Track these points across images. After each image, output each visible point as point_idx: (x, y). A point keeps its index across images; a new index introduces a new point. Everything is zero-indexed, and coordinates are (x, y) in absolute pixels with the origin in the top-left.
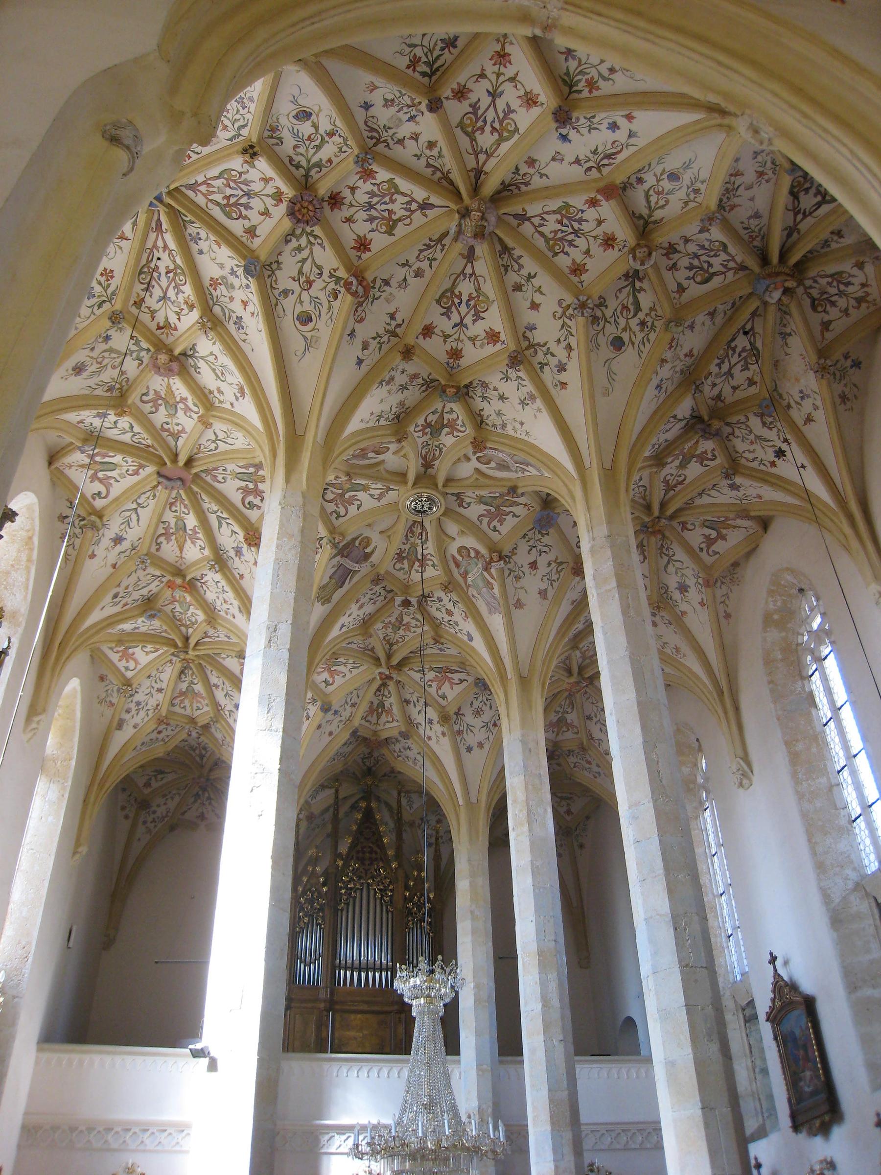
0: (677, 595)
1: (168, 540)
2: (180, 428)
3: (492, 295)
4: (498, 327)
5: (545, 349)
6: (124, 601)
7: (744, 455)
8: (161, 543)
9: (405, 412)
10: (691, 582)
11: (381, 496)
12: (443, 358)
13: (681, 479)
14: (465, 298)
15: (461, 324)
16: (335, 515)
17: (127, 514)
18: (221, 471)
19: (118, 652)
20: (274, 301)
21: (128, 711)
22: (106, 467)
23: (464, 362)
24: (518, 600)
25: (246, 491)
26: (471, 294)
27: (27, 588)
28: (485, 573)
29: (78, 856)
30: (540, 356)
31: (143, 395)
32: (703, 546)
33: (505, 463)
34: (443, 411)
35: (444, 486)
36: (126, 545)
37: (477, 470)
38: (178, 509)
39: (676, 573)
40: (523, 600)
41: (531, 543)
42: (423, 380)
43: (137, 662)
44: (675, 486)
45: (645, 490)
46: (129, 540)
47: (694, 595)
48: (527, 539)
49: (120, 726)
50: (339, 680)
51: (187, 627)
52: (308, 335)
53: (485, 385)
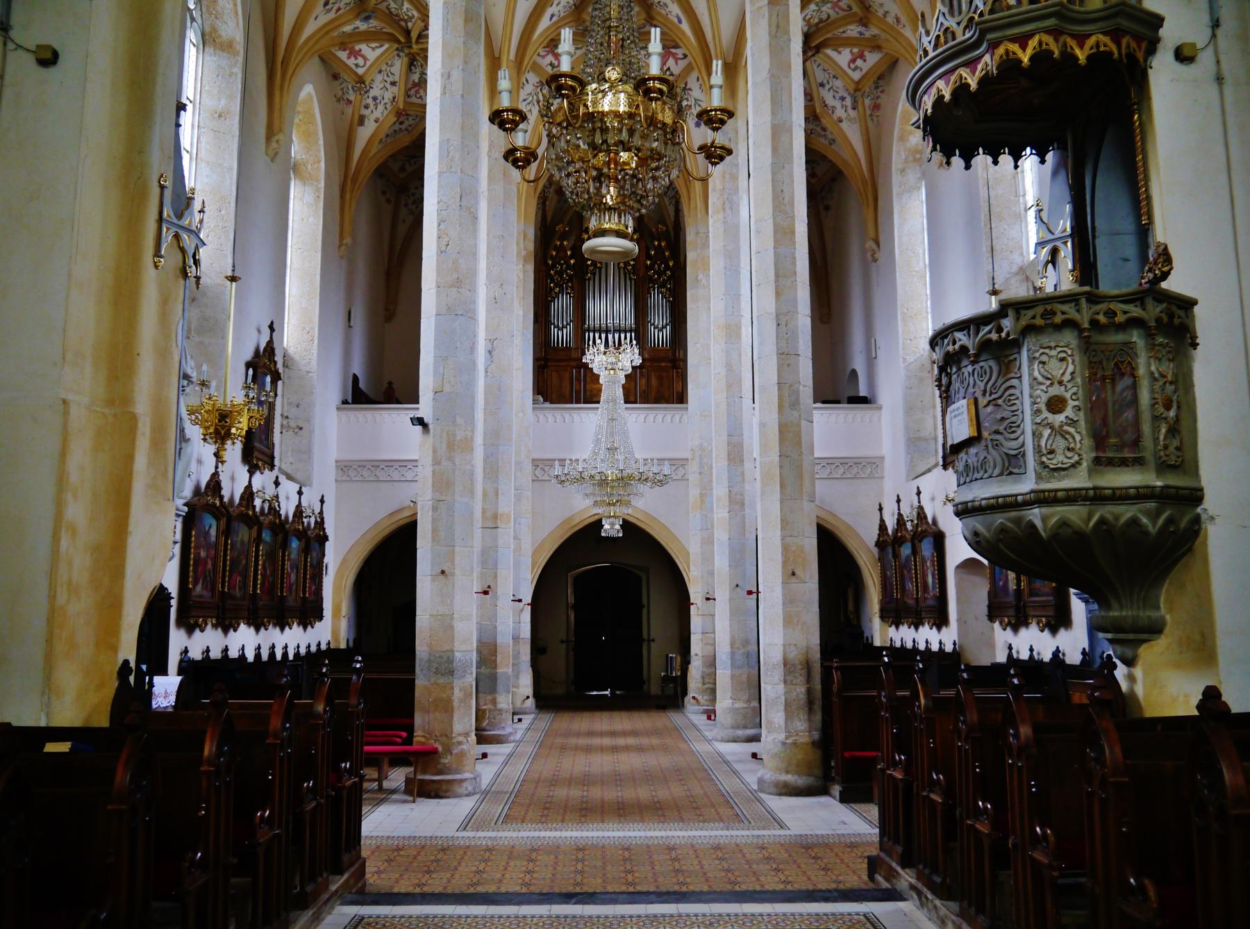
6: (336, 7)
21: (367, 107)
27: (237, 13)
29: (343, 248)
43: (365, 59)
49: (362, 120)
51: (406, 21)
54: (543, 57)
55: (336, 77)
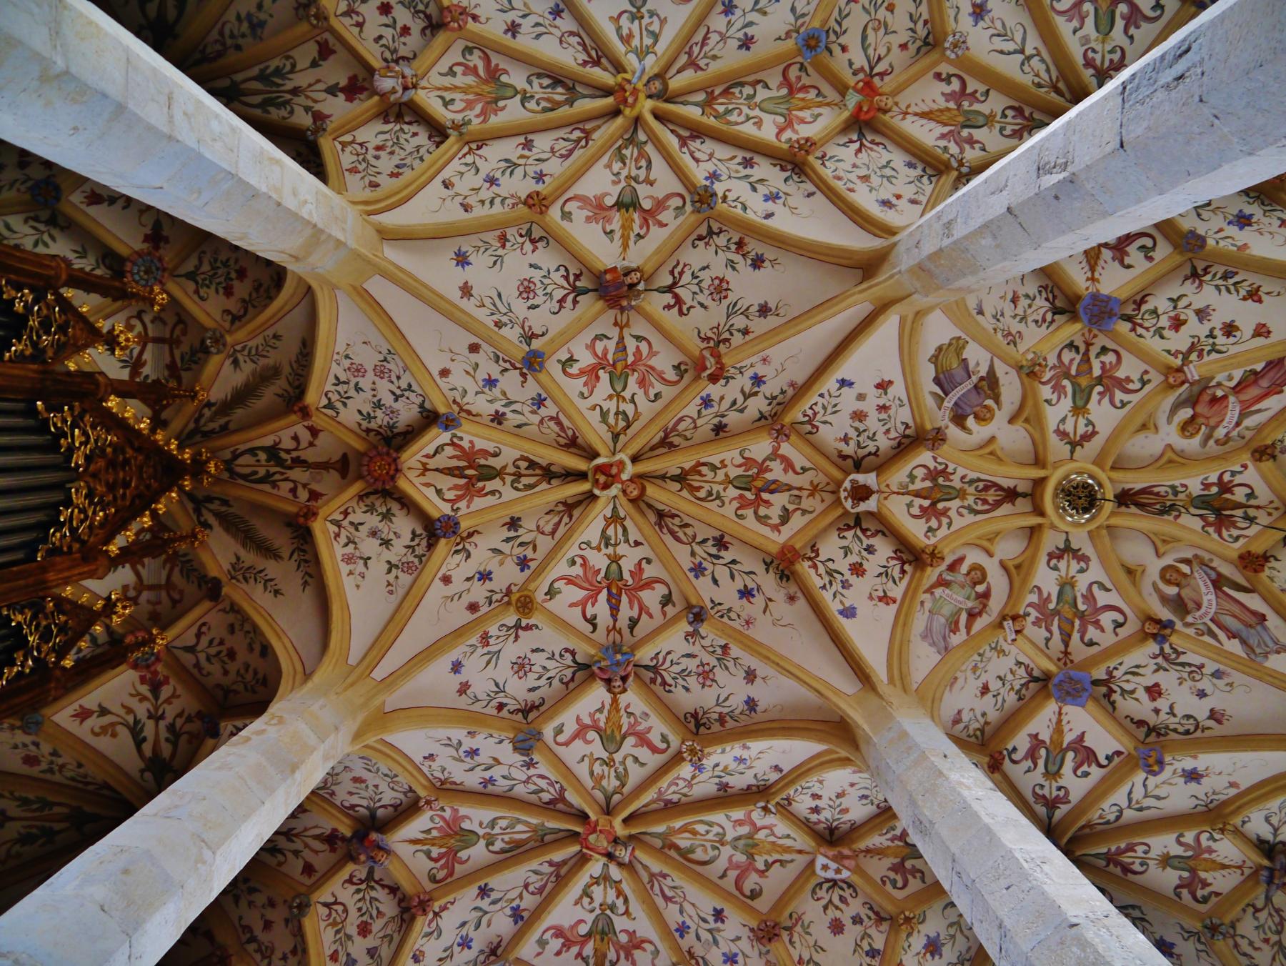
7: (1238, 939)
8: (949, 83)
11: (1062, 434)
13: (1136, 867)
22: (1104, 21)
33: (1191, 605)
38: (1009, 120)
39: (951, 925)
41: (1009, 677)
44: (1117, 863)
45: (1108, 822)
46: (972, 30)
48: (1015, 668)
50: (574, 386)
54: (591, 347)
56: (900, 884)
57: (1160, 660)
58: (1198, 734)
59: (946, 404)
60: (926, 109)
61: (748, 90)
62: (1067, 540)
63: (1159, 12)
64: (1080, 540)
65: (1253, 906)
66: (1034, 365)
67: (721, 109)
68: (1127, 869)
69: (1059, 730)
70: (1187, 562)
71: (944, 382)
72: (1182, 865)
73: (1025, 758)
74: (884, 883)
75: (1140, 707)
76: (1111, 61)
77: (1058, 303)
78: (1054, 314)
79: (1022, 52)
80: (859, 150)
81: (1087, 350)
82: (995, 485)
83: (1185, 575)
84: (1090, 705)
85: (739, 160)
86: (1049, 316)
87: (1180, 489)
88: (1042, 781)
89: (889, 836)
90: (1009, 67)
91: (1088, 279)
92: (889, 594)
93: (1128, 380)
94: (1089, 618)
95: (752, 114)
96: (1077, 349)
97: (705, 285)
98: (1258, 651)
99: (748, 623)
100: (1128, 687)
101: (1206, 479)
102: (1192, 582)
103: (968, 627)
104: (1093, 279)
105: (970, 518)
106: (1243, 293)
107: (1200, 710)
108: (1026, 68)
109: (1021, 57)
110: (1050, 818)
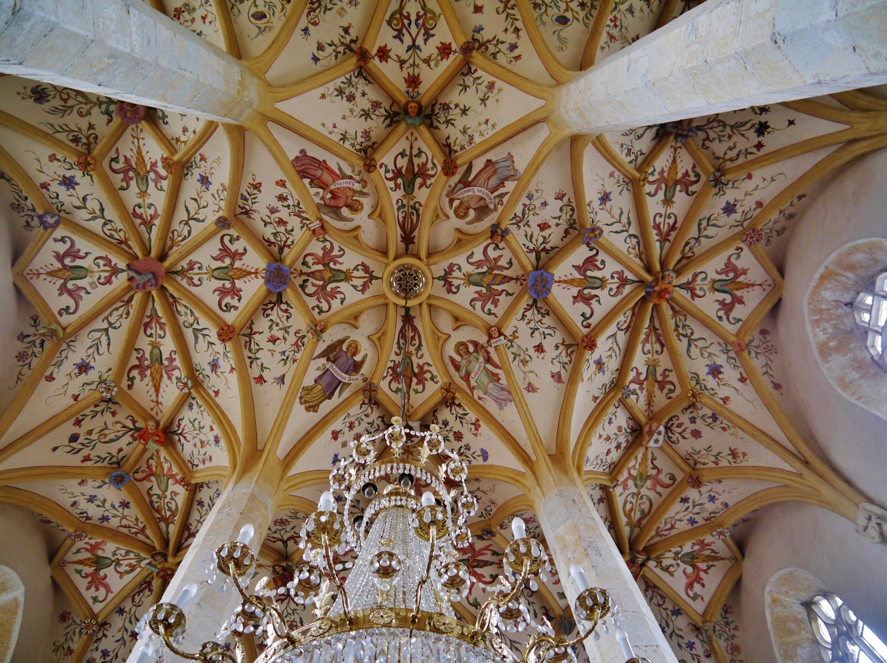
0: (711, 382)
1: (143, 376)
2: (152, 211)
3: (438, 11)
4: (448, 39)
5: (495, 42)
6: (85, 452)
7: (727, 157)
8: (134, 378)
9: (372, 147)
10: (721, 360)
11: (365, 287)
12: (403, 86)
13: (671, 221)
14: (413, 18)
15: (413, 47)
16: (317, 310)
17: (97, 335)
18: (196, 271)
19: (87, 576)
20: (230, 5)
22: (78, 273)
23: (422, 88)
24: (530, 384)
25: (223, 292)
26: (418, 13)
28: (489, 366)
30: (492, 49)
31: (113, 160)
32: (721, 313)
33: (482, 203)
34: (411, 153)
35: (427, 258)
36: (92, 375)
37: (458, 230)
38: (153, 331)
39: (702, 354)
40: (535, 384)
41: (532, 325)
42: (386, 110)
44: (668, 234)
45: (638, 243)
47: (730, 374)
52: (263, 26)
53: (446, 107)
55: (64, 617)
56: (672, 387)
57: (521, 224)
58: (574, 205)
59: (346, 381)
60: (153, 389)
61: (155, 498)
62: (438, 278)
63: (66, 239)
64: (439, 270)
65: (704, 140)
66: (316, 331)
67: (168, 513)
68: (673, 228)
69: (571, 282)
70: (451, 201)
71: (331, 387)
72: (672, 190)
73: (589, 305)
74: (670, 398)
75: (555, 236)
76: (105, 265)
77: (274, 299)
78: (282, 302)
79: (106, 330)
80: (185, 438)
81: (306, 274)
82: (401, 331)
83: (461, 203)
84: (551, 270)
85: (199, 508)
86: (284, 307)
87: (400, 204)
88: (607, 290)
89: (639, 392)
90: (119, 337)
91: (256, 277)
92: (473, 421)
93: (324, 248)
94: (493, 265)
95: (169, 497)
96: (305, 281)
97: (280, 528)
98: (512, 173)
99: (493, 503)
100: (541, 240)
101: (391, 189)
102: (466, 199)
103: (496, 366)
104: (256, 273)
105: (424, 349)
106: (255, 191)
107: (555, 206)
108: (117, 325)
109: (110, 329)
110: (634, 282)
